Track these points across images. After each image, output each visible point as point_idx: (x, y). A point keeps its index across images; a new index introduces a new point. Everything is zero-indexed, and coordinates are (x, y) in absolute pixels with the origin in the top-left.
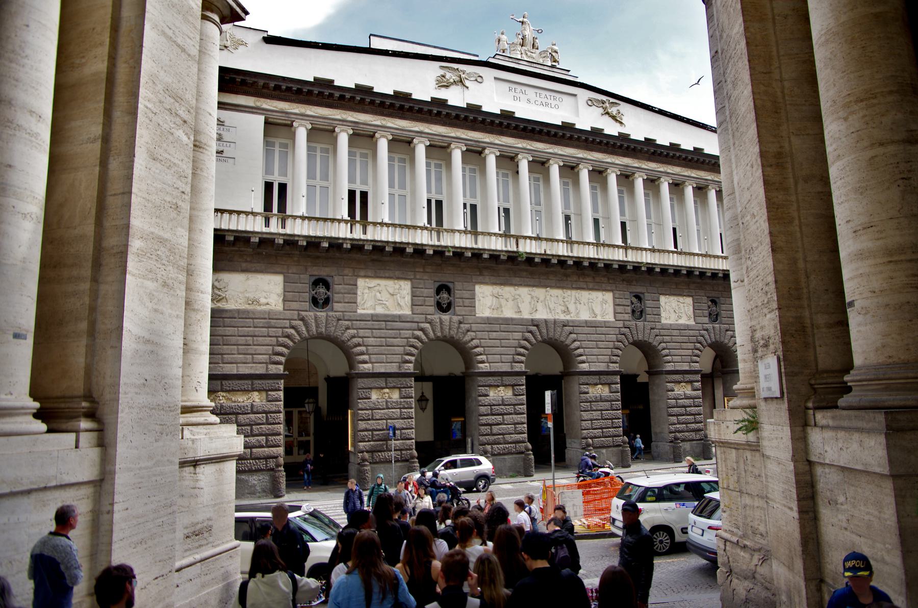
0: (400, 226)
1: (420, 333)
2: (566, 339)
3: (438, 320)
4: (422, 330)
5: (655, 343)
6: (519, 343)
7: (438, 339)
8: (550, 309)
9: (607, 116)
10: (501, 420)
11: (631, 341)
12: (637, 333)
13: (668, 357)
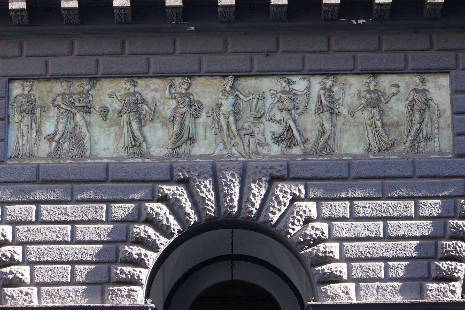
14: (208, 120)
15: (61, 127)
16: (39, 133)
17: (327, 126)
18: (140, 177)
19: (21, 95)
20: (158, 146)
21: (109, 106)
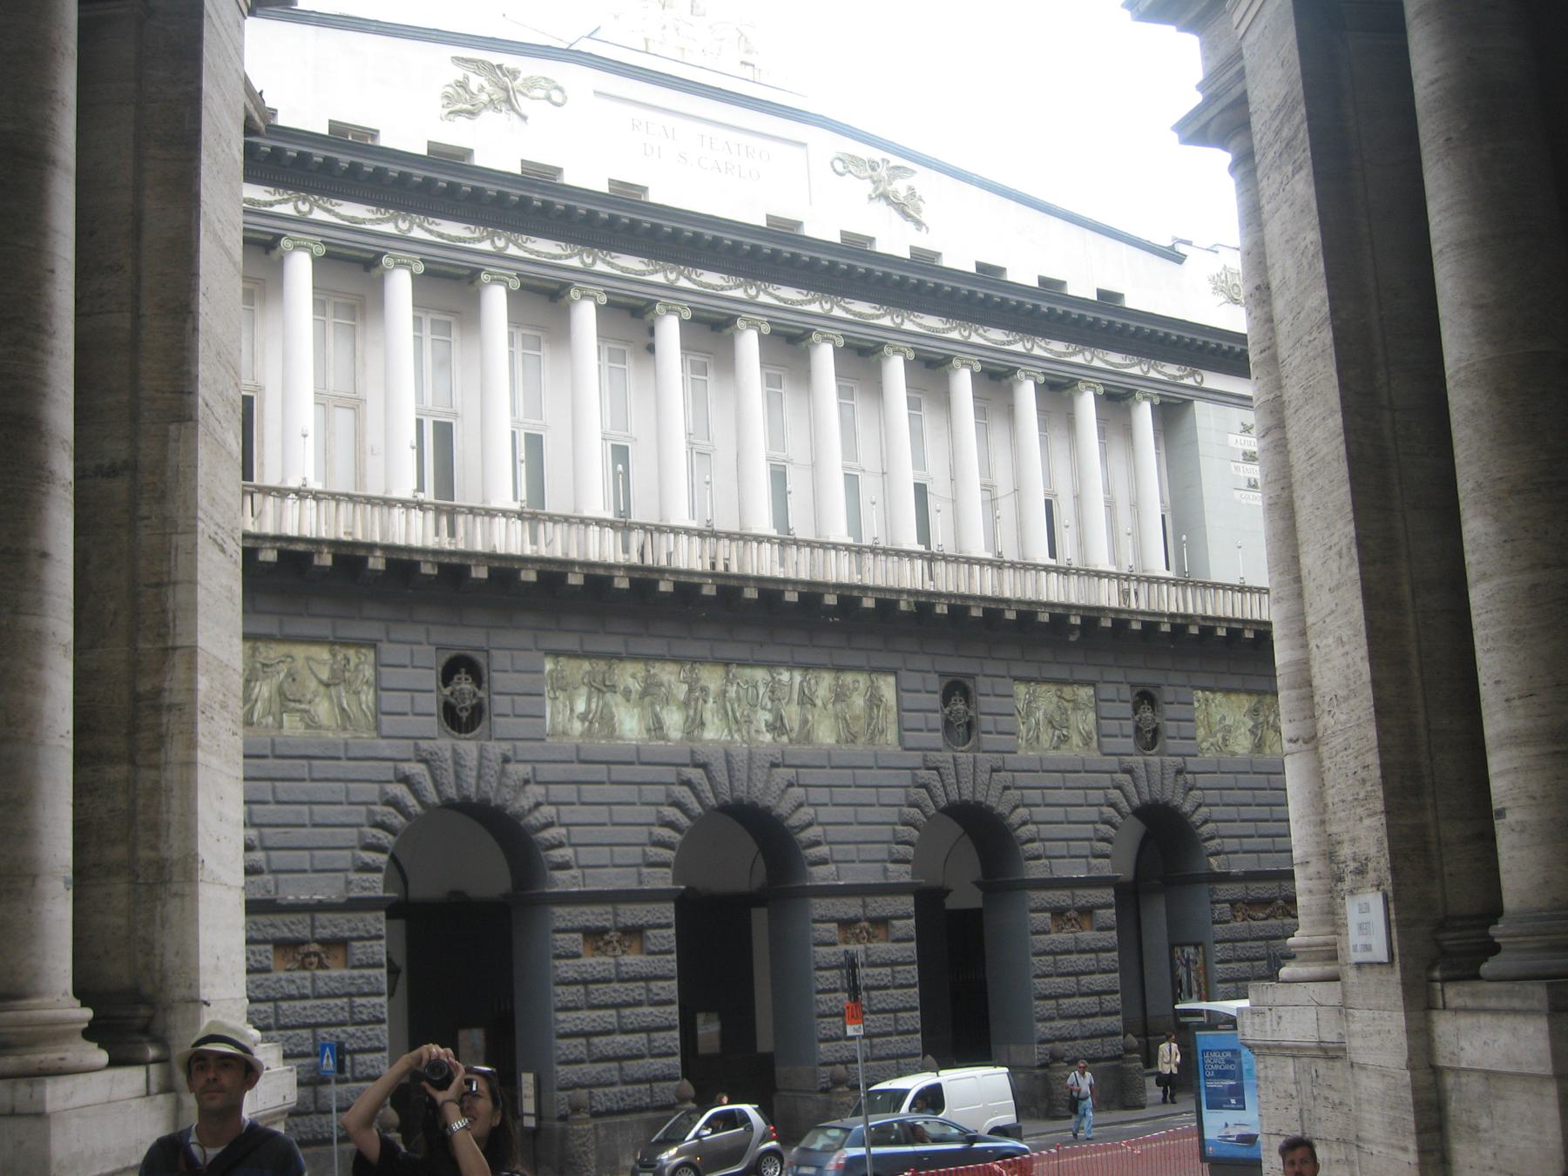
0: (351, 498)
1: (400, 790)
2: (780, 801)
3: (448, 754)
4: (406, 780)
5: (1002, 809)
6: (659, 812)
7: (449, 805)
8: (737, 722)
9: (883, 203)
10: (614, 1020)
11: (943, 803)
12: (958, 782)
13: (1035, 845)
14: (715, 705)
15: (593, 706)
16: (572, 710)
17: (810, 718)
18: (666, 760)
19: (555, 670)
20: (675, 730)
21: (632, 687)
